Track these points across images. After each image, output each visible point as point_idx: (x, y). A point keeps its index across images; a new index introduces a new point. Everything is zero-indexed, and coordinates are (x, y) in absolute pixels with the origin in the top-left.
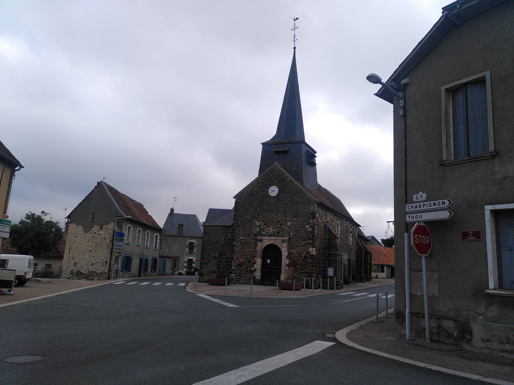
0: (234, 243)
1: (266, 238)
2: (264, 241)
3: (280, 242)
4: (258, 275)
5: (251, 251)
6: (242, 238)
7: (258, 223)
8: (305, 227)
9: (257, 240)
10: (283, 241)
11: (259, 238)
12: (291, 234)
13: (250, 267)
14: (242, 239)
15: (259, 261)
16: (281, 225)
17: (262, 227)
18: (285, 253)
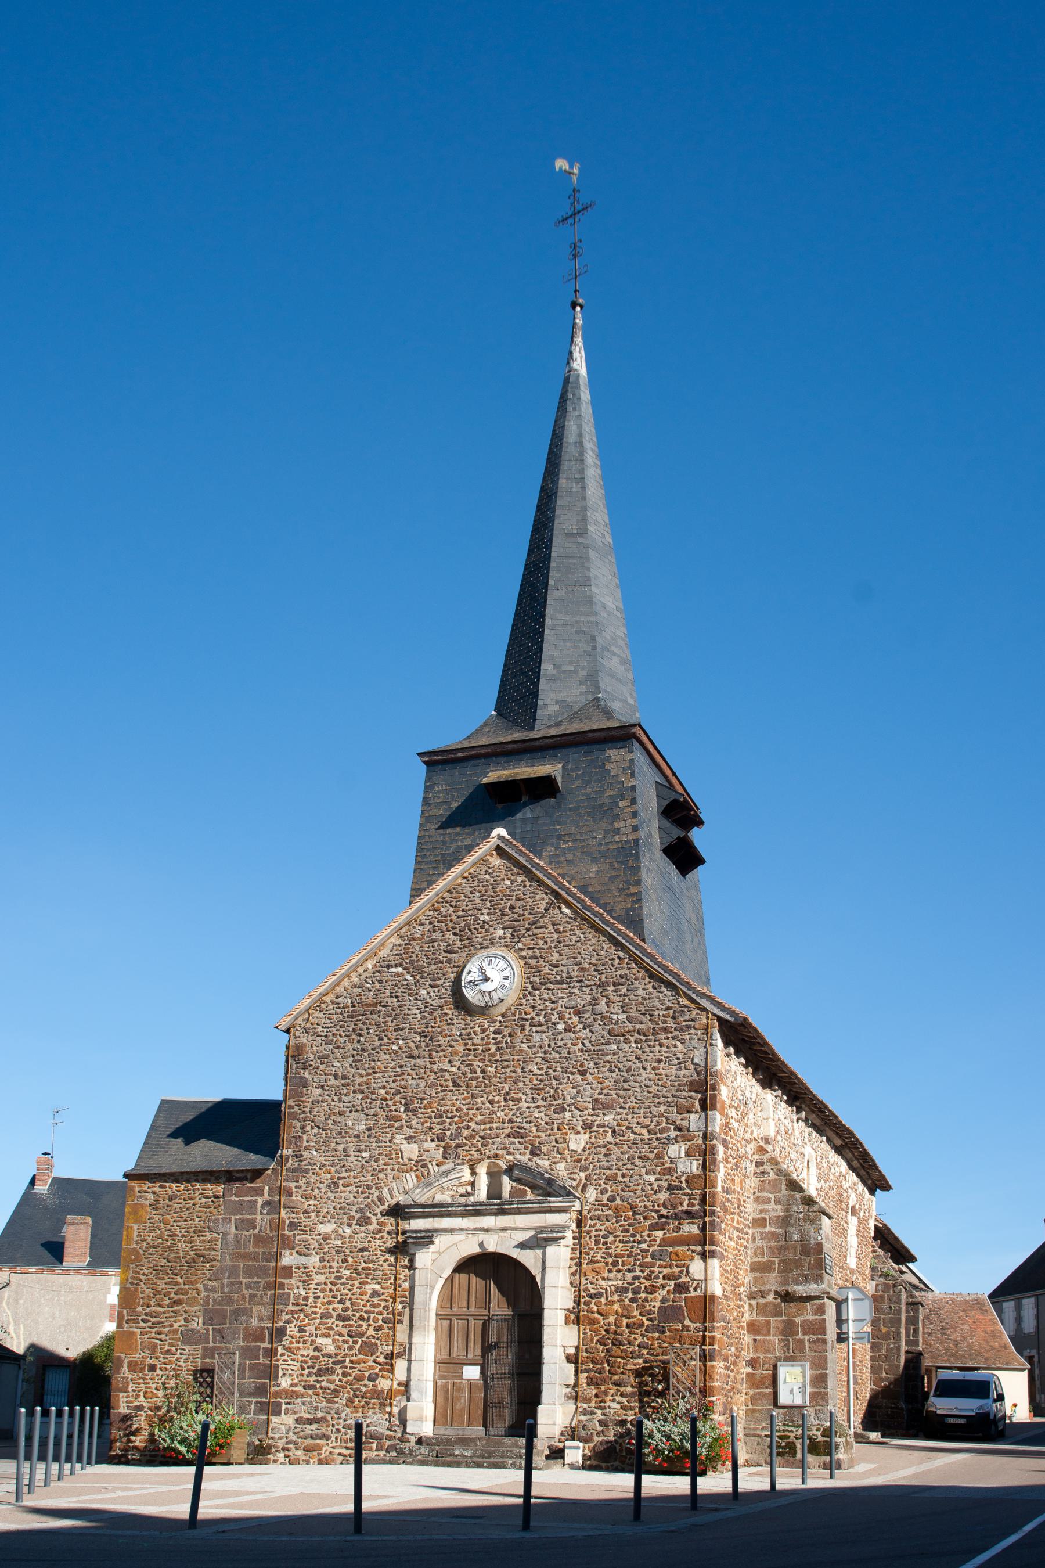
0: (288, 1259)
5: (375, 1293)
6: (327, 1228)
7: (411, 1151)
18: (557, 1298)
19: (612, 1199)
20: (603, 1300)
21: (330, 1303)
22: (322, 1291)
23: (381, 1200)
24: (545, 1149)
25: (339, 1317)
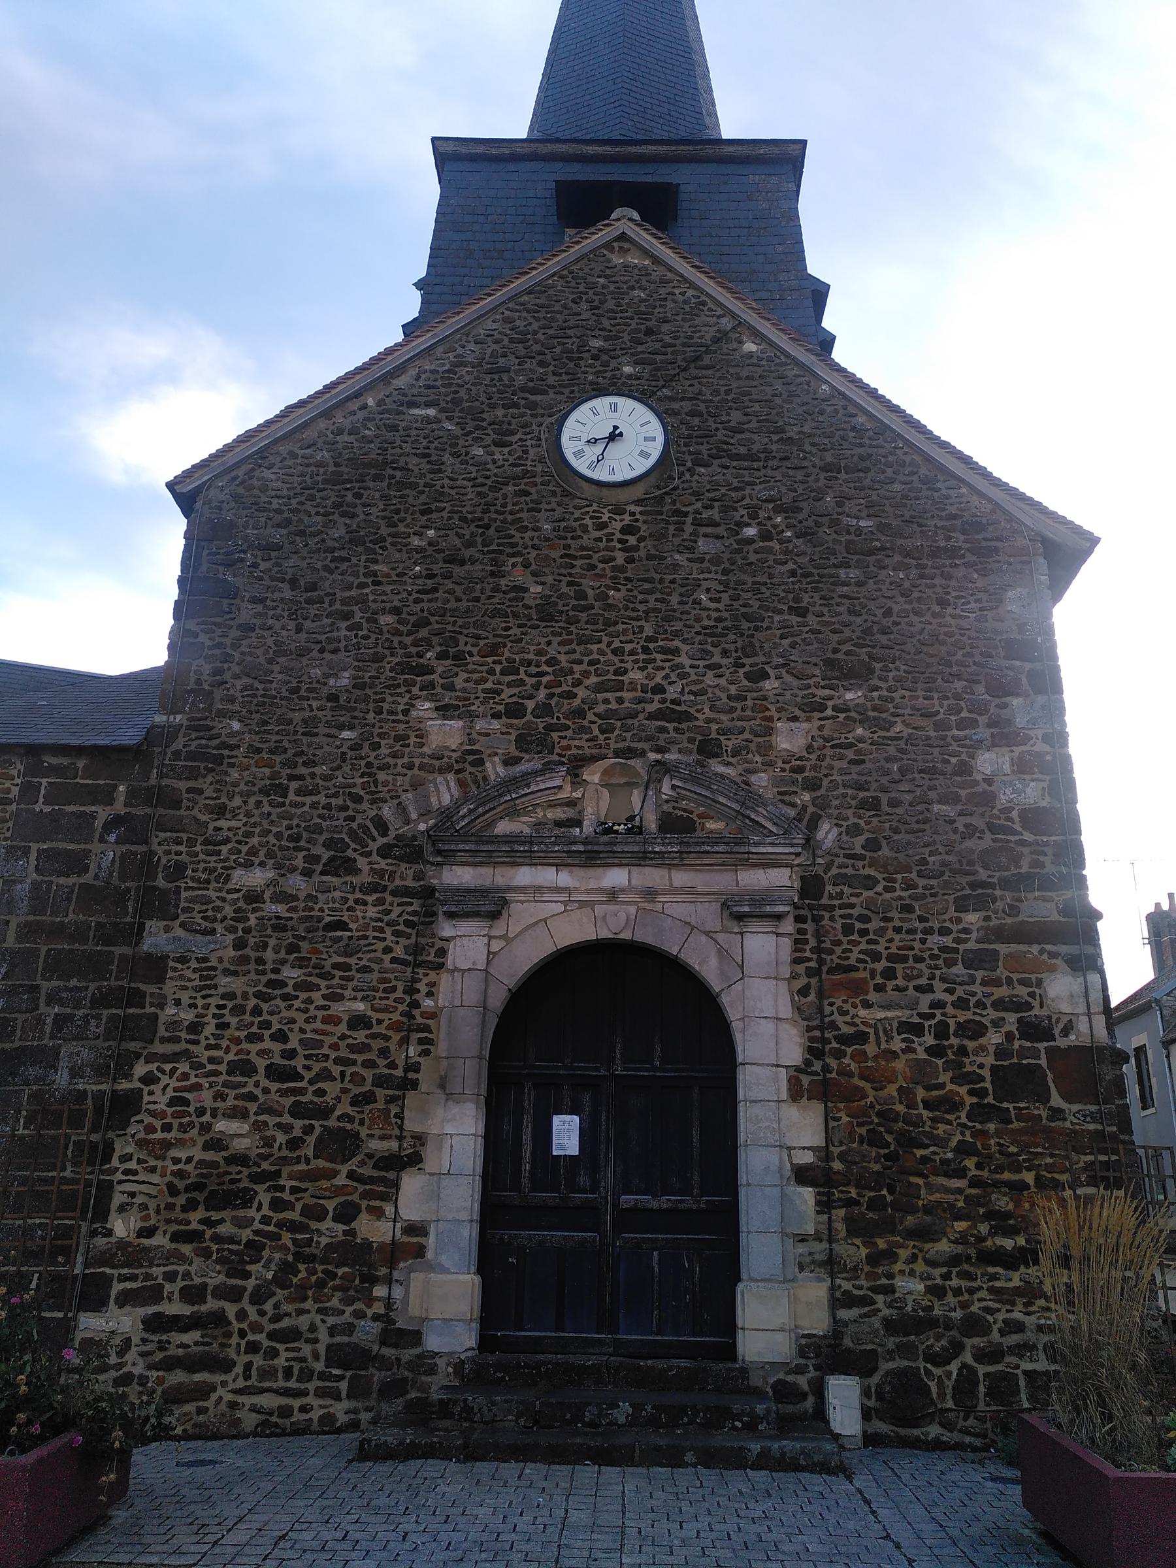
0: (157, 938)
1: (547, 876)
2: (521, 914)
3: (708, 914)
4: (445, 1301)
5: (358, 1022)
6: (257, 878)
7: (446, 734)
8: (964, 769)
9: (430, 903)
10: (742, 912)
11: (461, 876)
12: (827, 834)
13: (347, 1214)
14: (254, 897)
15: (456, 1132)
16: (708, 749)
17: (495, 770)
18: (767, 1034)
19: (872, 845)
20: (871, 1049)
21: (253, 1038)
22: (238, 1010)
23: (382, 826)
24: (729, 744)
25: (273, 1072)
